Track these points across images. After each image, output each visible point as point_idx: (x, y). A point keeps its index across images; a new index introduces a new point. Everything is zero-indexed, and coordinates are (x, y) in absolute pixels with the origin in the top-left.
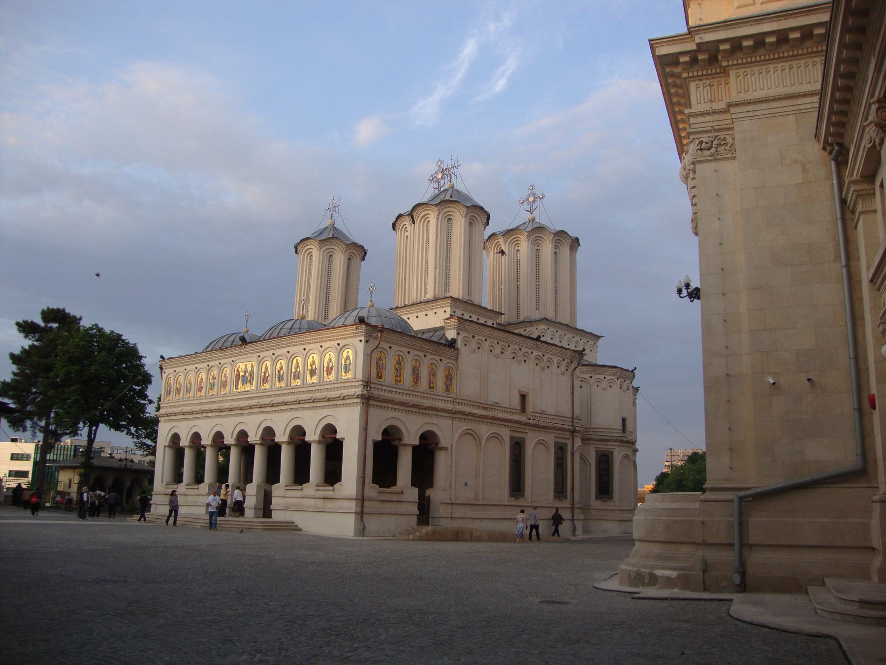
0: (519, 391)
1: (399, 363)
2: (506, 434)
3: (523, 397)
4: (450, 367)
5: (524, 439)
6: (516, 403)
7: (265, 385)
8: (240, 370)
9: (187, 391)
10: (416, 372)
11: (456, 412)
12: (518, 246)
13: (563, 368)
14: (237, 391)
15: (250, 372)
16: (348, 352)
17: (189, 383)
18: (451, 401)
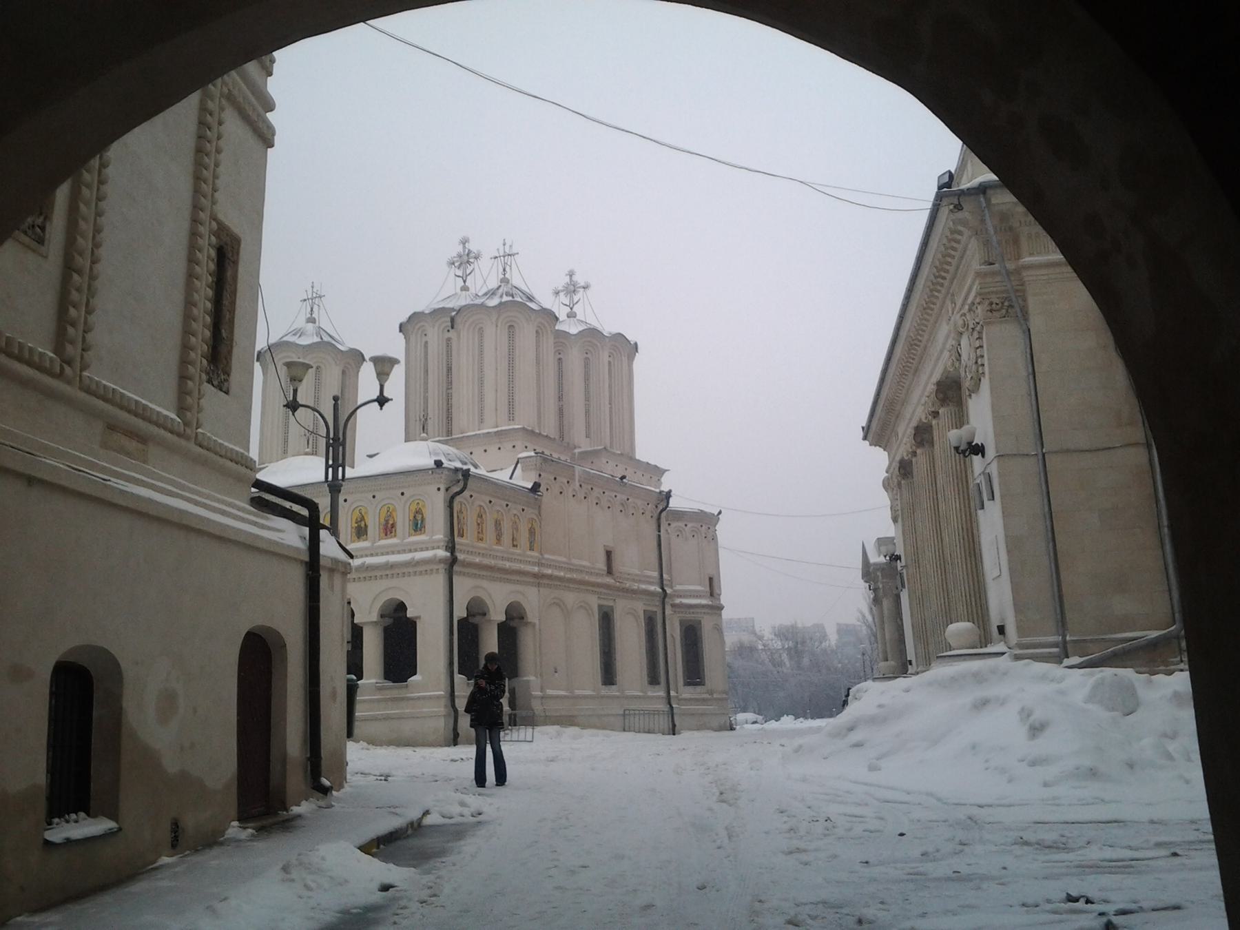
0: (604, 546)
1: (480, 516)
2: (594, 601)
3: (609, 554)
4: (533, 519)
5: (612, 608)
6: (601, 565)
10: (498, 524)
11: (544, 576)
12: (560, 354)
13: (648, 514)
16: (418, 503)
18: (536, 562)
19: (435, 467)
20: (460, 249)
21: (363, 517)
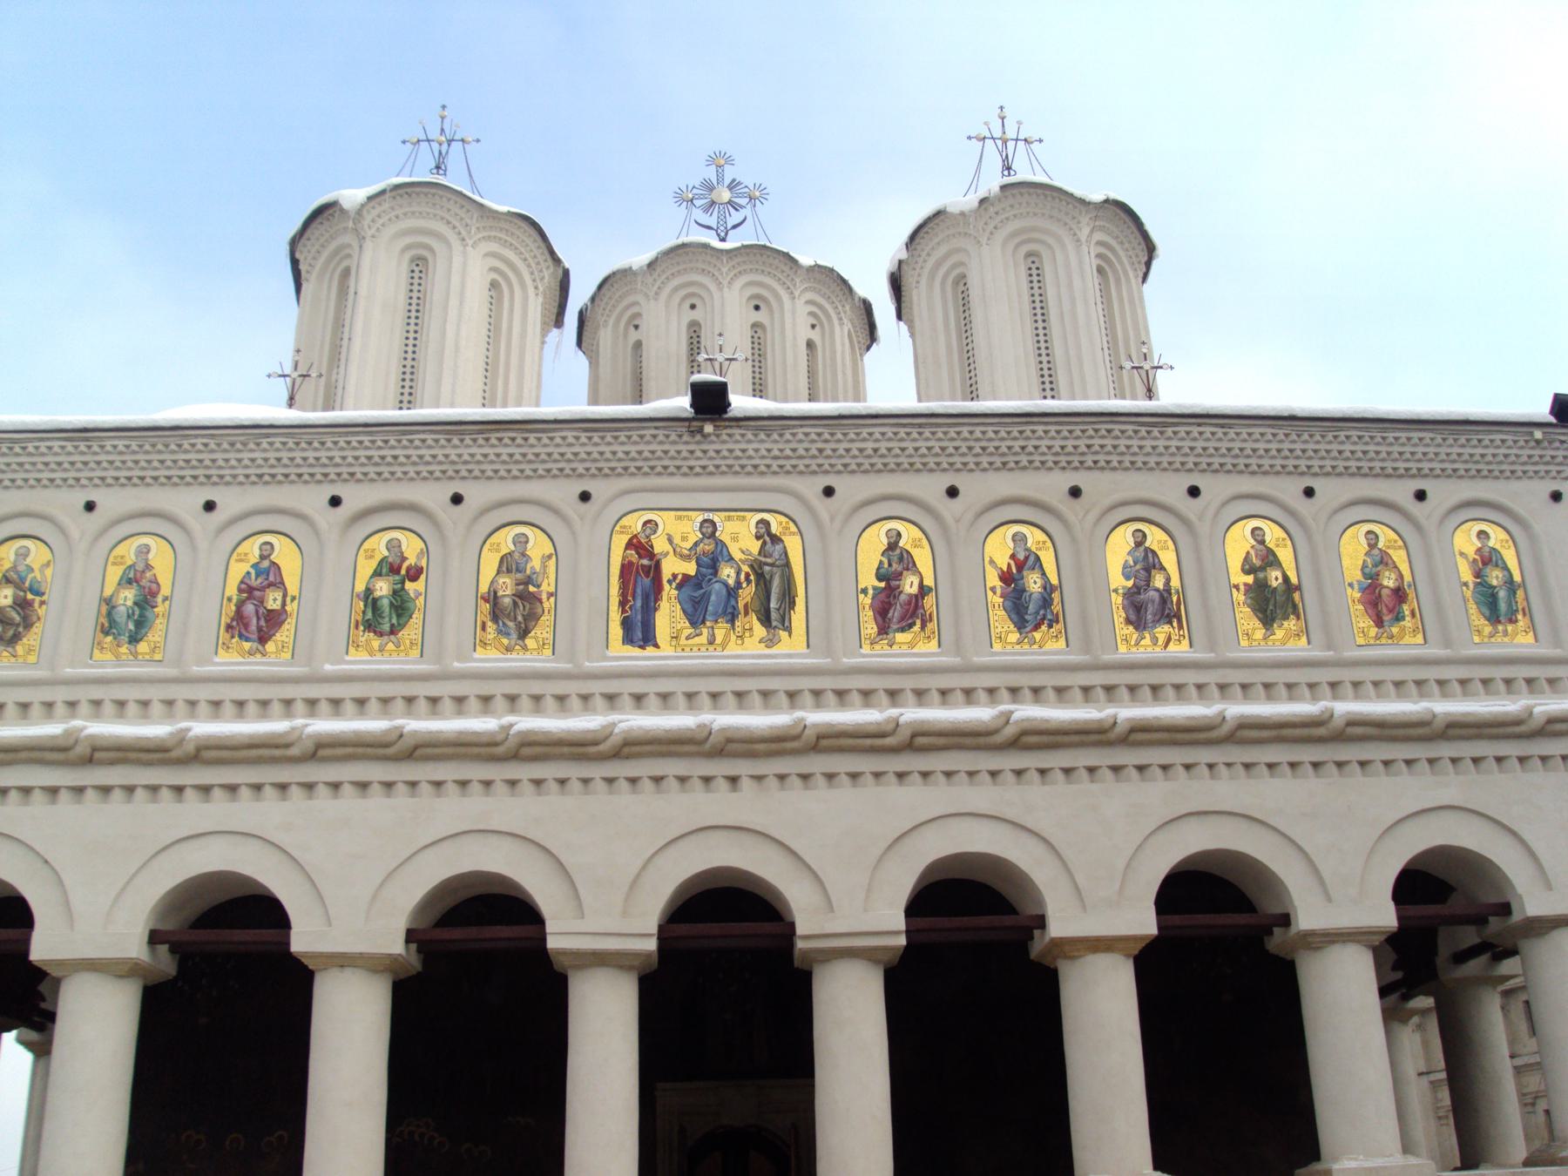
7: (900, 637)
8: (660, 545)
9: (109, 626)
14: (650, 651)
17: (128, 580)
19: (1553, 420)
20: (711, 174)
21: (1270, 552)
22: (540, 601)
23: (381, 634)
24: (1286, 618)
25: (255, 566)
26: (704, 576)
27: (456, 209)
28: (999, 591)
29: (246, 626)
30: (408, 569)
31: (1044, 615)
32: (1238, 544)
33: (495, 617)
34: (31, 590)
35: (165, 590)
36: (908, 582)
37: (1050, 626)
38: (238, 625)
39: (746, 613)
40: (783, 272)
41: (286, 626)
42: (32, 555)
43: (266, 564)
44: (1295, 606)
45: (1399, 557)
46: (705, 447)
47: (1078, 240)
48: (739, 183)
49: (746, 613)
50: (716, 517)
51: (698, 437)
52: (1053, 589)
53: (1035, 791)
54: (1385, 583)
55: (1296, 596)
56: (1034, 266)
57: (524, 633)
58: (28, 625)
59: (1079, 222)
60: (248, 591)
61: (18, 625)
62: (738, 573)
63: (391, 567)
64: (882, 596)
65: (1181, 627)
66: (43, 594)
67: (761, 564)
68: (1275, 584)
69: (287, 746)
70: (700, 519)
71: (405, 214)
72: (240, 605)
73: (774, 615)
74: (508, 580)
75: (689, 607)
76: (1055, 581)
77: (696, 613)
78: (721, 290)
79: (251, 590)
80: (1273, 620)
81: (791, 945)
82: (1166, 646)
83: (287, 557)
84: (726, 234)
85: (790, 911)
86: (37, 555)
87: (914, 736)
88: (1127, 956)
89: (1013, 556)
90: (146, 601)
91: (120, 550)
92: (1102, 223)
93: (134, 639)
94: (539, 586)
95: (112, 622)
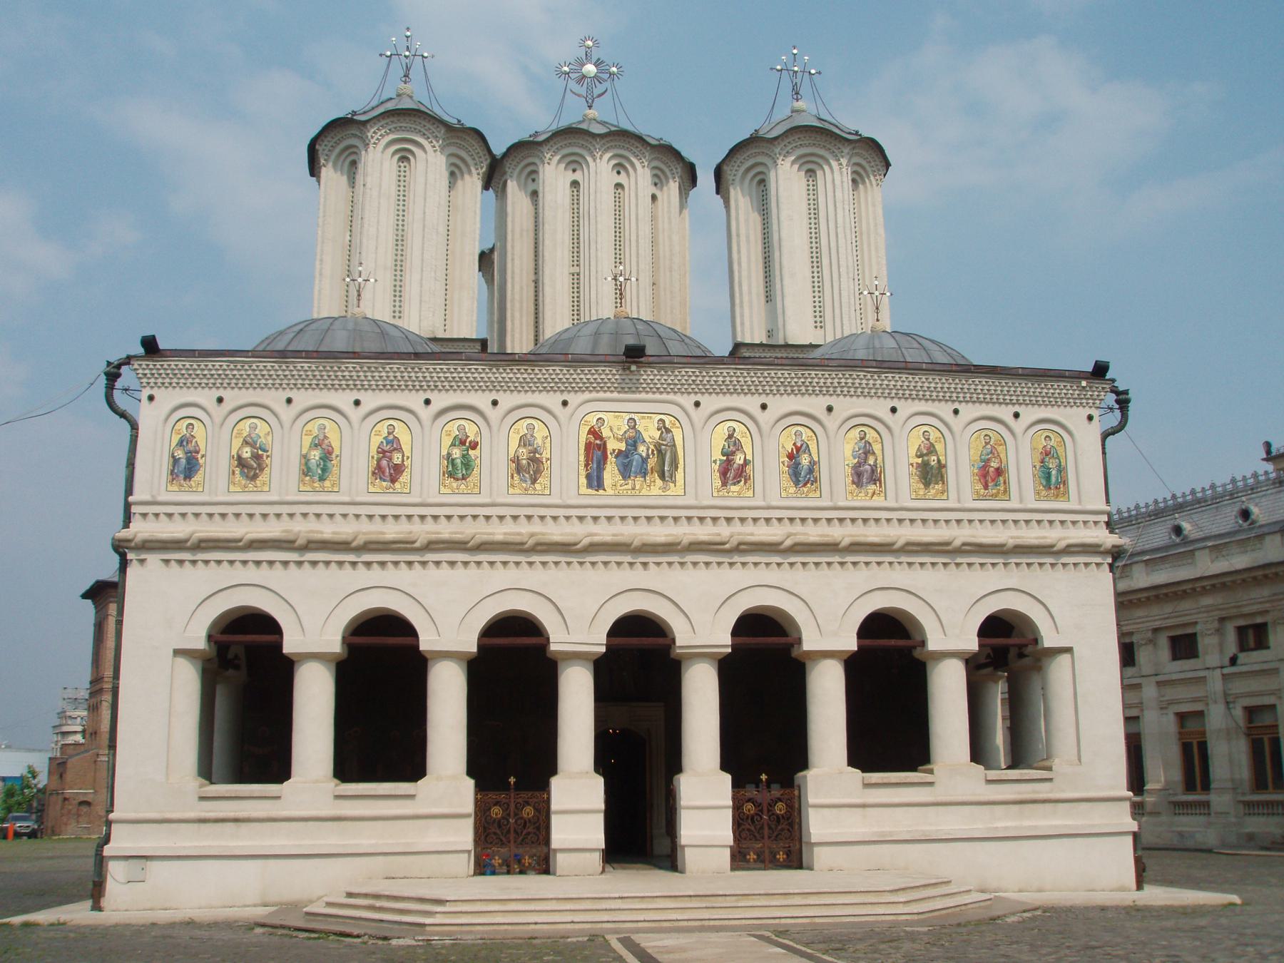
7: (734, 488)
8: (606, 433)
9: (306, 471)
14: (601, 492)
15: (658, 447)
17: (316, 445)
21: (932, 445)
22: (542, 462)
23: (458, 480)
24: (937, 483)
25: (385, 438)
26: (630, 451)
27: (428, 126)
28: (786, 464)
29: (383, 473)
30: (470, 442)
31: (809, 480)
32: (916, 441)
33: (518, 473)
34: (261, 448)
35: (337, 452)
36: (738, 457)
37: (812, 484)
38: (378, 472)
39: (652, 473)
40: (637, 147)
41: (405, 474)
42: (259, 428)
43: (391, 437)
44: (942, 477)
45: (1000, 449)
46: (630, 377)
47: (841, 164)
48: (602, 62)
49: (652, 473)
50: (636, 417)
51: (628, 372)
52: (815, 463)
53: (799, 573)
54: (992, 464)
55: (944, 470)
56: (811, 179)
57: (534, 481)
58: (262, 470)
59: (842, 152)
60: (383, 452)
61: (256, 469)
62: (648, 450)
63: (461, 442)
64: (724, 465)
65: (881, 486)
66: (268, 451)
67: (661, 445)
68: (933, 463)
69: (413, 542)
70: (628, 418)
71: (395, 128)
72: (379, 461)
73: (667, 474)
74: (524, 450)
75: (622, 468)
76: (816, 459)
77: (625, 472)
78: (594, 160)
79: (384, 452)
80: (930, 484)
81: (672, 651)
82: (873, 496)
83: (401, 433)
84: (593, 101)
85: (672, 632)
86: (262, 428)
87: (740, 544)
88: (841, 659)
89: (794, 444)
90: (327, 458)
91: (309, 427)
92: (857, 151)
93: (322, 479)
94: (541, 454)
95: (309, 469)
